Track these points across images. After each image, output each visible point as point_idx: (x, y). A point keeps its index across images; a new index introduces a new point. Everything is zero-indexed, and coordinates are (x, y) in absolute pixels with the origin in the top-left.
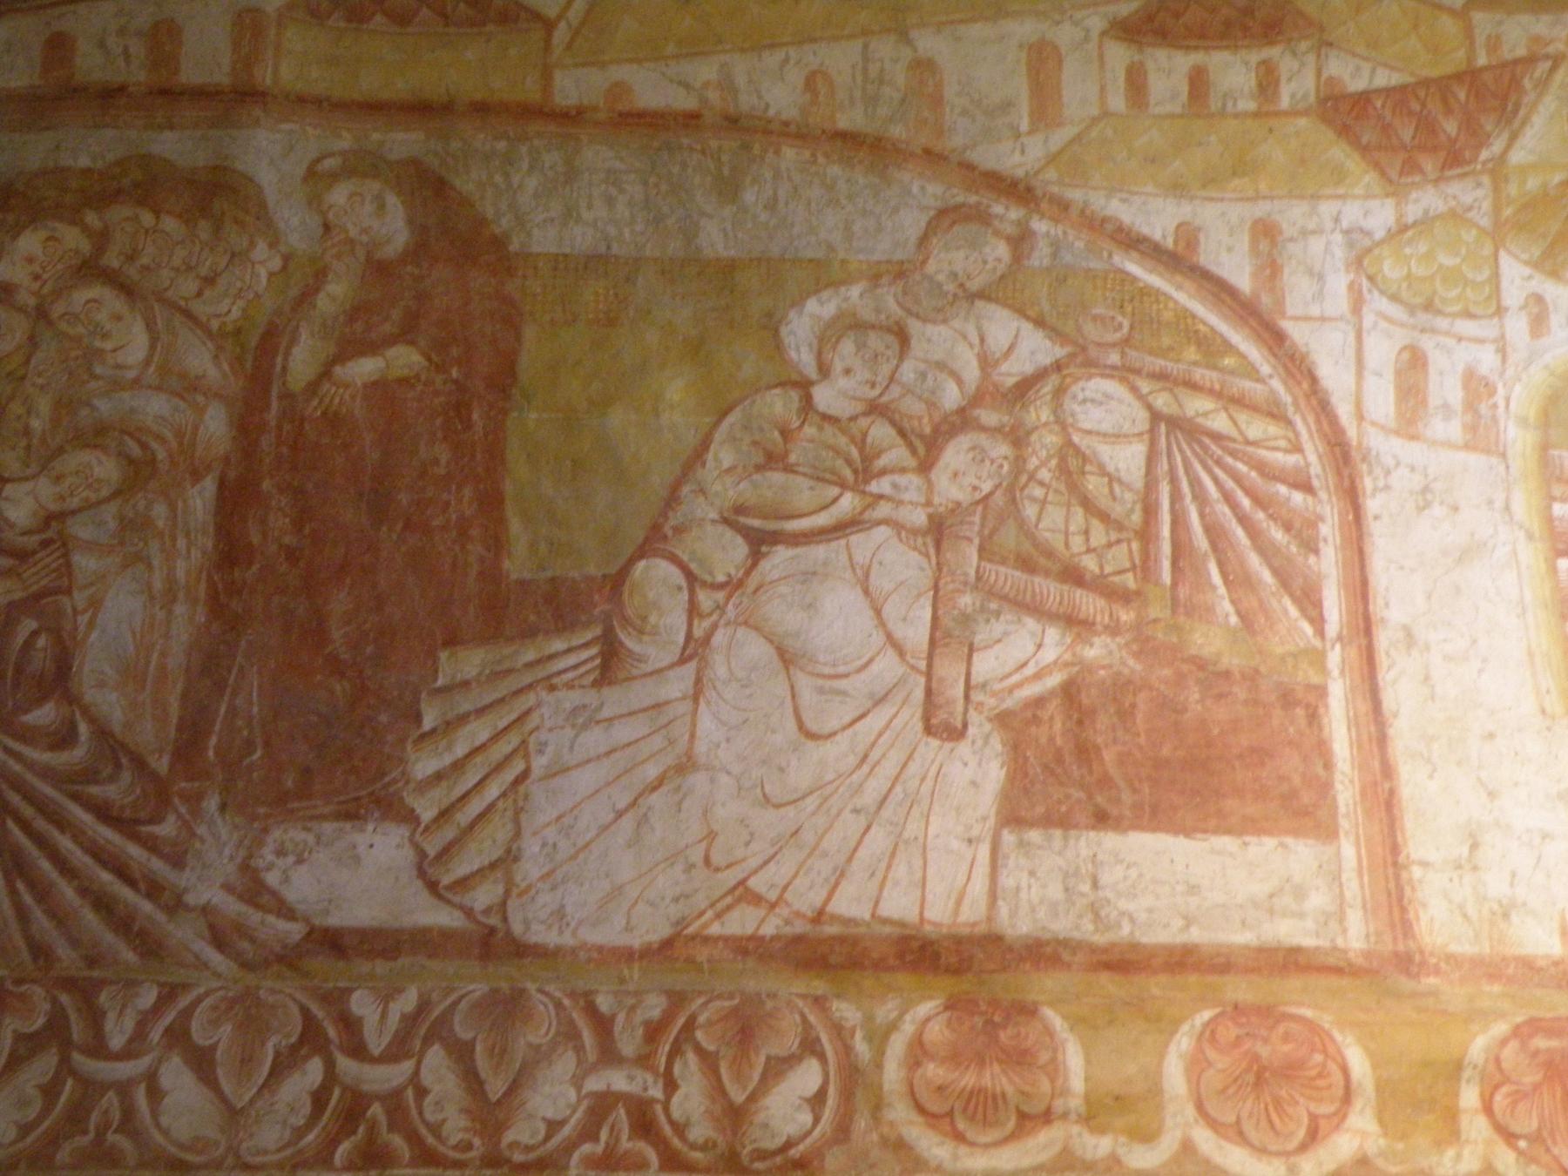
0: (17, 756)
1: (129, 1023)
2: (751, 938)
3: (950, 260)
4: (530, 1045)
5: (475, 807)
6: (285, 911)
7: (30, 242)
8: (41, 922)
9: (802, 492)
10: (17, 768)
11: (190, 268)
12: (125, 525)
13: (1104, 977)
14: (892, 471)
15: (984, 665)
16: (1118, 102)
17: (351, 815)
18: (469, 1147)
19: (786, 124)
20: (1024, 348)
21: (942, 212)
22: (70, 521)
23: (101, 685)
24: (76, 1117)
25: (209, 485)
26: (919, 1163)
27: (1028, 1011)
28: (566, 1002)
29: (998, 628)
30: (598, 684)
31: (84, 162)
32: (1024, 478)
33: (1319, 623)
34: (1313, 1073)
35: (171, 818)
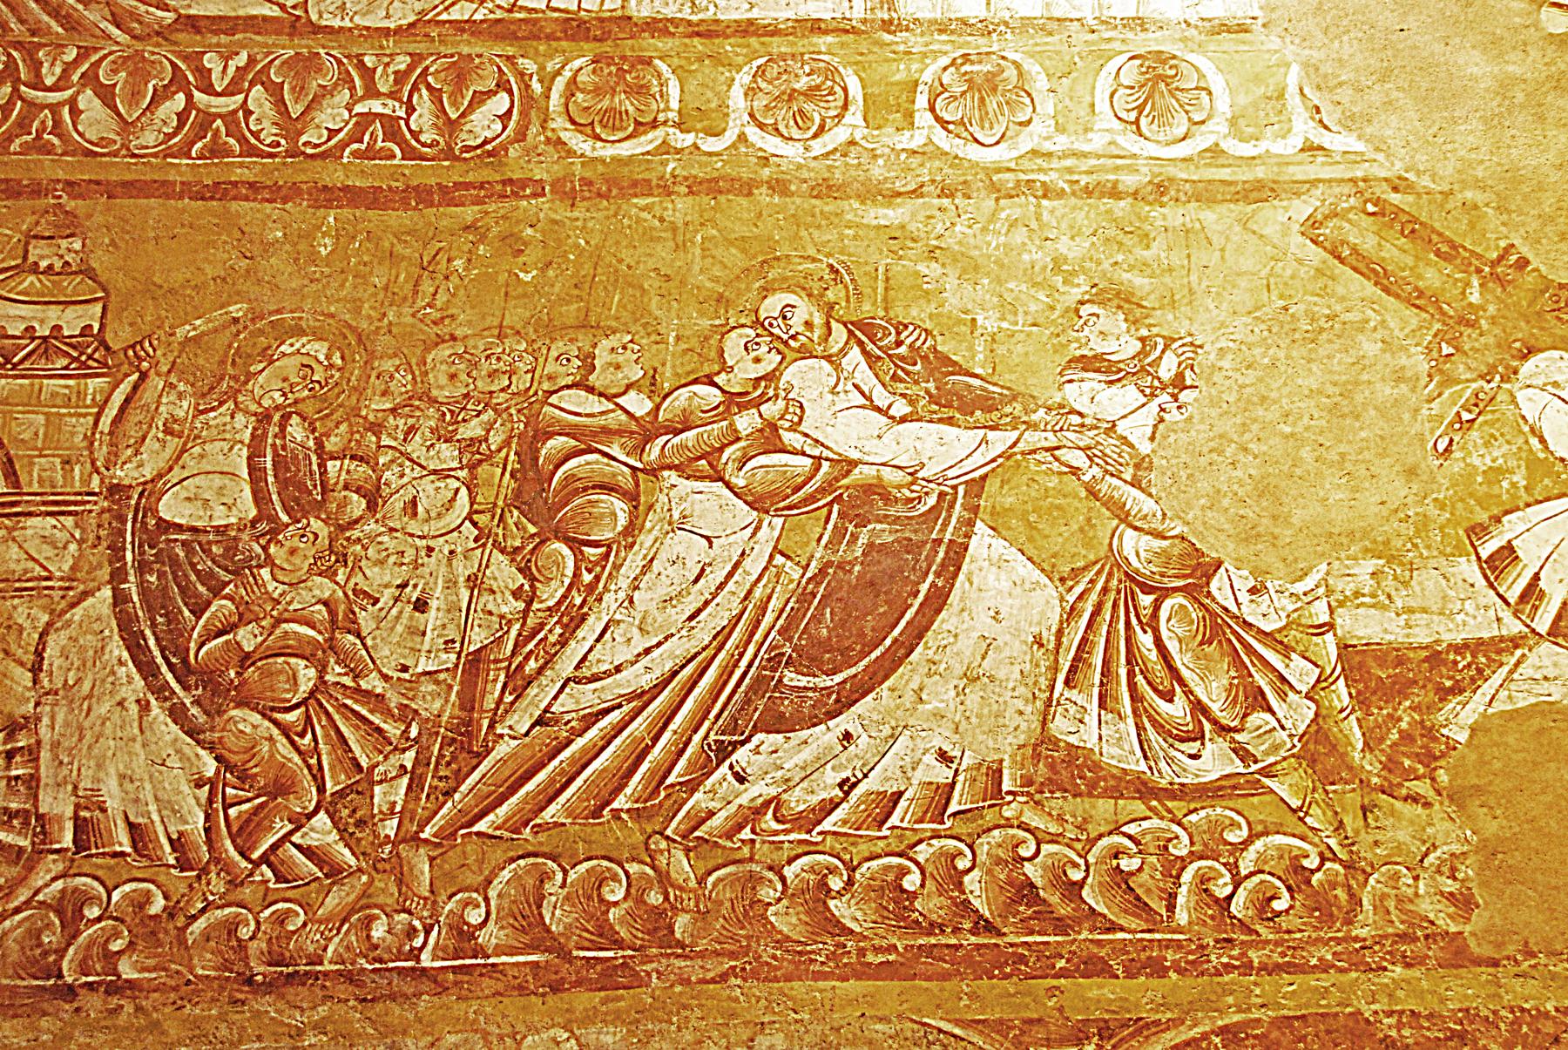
1: (58, 70)
18: (278, 144)
26: (571, 153)
27: (648, 62)
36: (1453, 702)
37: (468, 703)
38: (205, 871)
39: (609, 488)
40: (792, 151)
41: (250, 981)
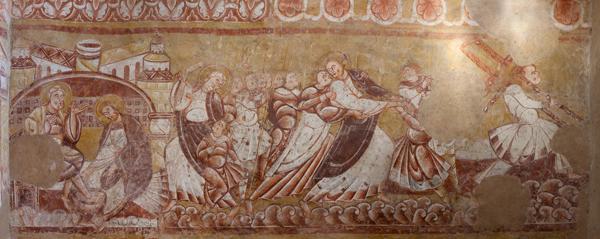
24: (147, 11)
36: (479, 174)
37: (259, 168)
38: (204, 205)
39: (290, 115)
40: (335, 20)
41: (215, 229)
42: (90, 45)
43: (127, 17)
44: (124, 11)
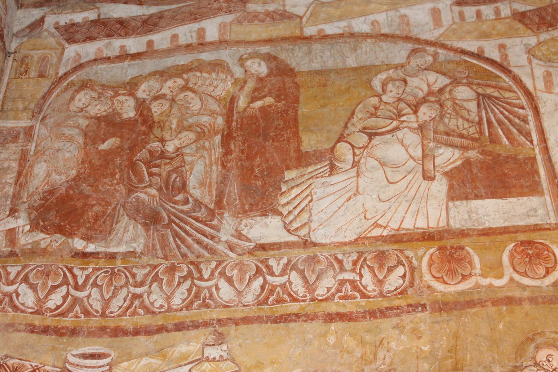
0: (174, 208)
1: (209, 271)
2: (380, 236)
3: (416, 62)
4: (320, 269)
5: (298, 210)
6: (248, 240)
7: (169, 83)
8: (184, 249)
9: (381, 122)
10: (174, 211)
11: (211, 85)
12: (197, 150)
13: (483, 238)
14: (406, 115)
15: (438, 161)
16: (457, 20)
17: (265, 214)
18: (306, 296)
19: (367, 34)
20: (439, 81)
21: (413, 51)
22: (183, 149)
23: (194, 188)
24: (197, 296)
25: (219, 137)
27: (462, 248)
28: (329, 257)
29: (441, 151)
30: (330, 175)
31: (182, 63)
32: (444, 113)
33: (531, 142)
34: (546, 256)
35: (216, 220)
42: (92, 356)
43: (161, 306)
44: (157, 299)
